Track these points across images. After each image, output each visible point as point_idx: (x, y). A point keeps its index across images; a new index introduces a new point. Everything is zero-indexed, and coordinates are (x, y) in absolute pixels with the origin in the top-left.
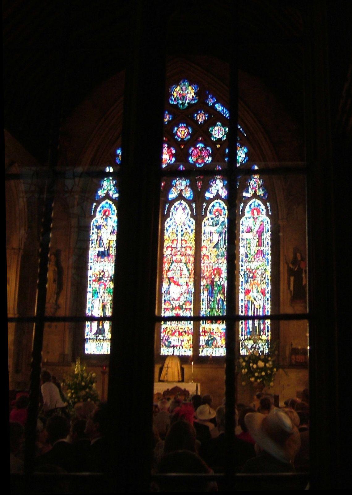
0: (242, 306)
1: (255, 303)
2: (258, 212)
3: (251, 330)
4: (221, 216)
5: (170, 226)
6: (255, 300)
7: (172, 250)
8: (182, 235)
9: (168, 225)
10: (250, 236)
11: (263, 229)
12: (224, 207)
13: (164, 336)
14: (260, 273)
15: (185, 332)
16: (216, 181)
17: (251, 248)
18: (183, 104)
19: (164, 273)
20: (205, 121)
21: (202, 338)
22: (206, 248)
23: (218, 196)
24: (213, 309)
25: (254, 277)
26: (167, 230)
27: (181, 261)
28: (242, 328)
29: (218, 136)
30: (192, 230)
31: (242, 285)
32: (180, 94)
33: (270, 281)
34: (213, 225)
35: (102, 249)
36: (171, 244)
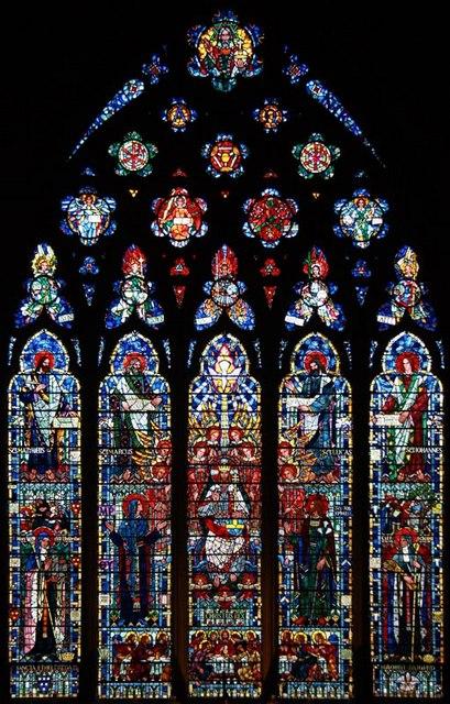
0: (375, 584)
1: (407, 578)
3: (397, 639)
4: (324, 372)
5: (200, 396)
6: (407, 571)
7: (206, 454)
8: (231, 418)
9: (198, 391)
10: (393, 420)
12: (330, 350)
13: (194, 655)
14: (418, 508)
15: (244, 644)
16: (311, 284)
17: (398, 450)
20: (281, 124)
21: (283, 659)
22: (290, 447)
23: (315, 323)
24: (307, 591)
25: (402, 519)
26: (195, 405)
27: (229, 481)
28: (376, 636)
29: (315, 168)
30: (254, 406)
31: (375, 536)
32: (216, 50)
33: (441, 527)
34: (304, 395)
36: (205, 439)
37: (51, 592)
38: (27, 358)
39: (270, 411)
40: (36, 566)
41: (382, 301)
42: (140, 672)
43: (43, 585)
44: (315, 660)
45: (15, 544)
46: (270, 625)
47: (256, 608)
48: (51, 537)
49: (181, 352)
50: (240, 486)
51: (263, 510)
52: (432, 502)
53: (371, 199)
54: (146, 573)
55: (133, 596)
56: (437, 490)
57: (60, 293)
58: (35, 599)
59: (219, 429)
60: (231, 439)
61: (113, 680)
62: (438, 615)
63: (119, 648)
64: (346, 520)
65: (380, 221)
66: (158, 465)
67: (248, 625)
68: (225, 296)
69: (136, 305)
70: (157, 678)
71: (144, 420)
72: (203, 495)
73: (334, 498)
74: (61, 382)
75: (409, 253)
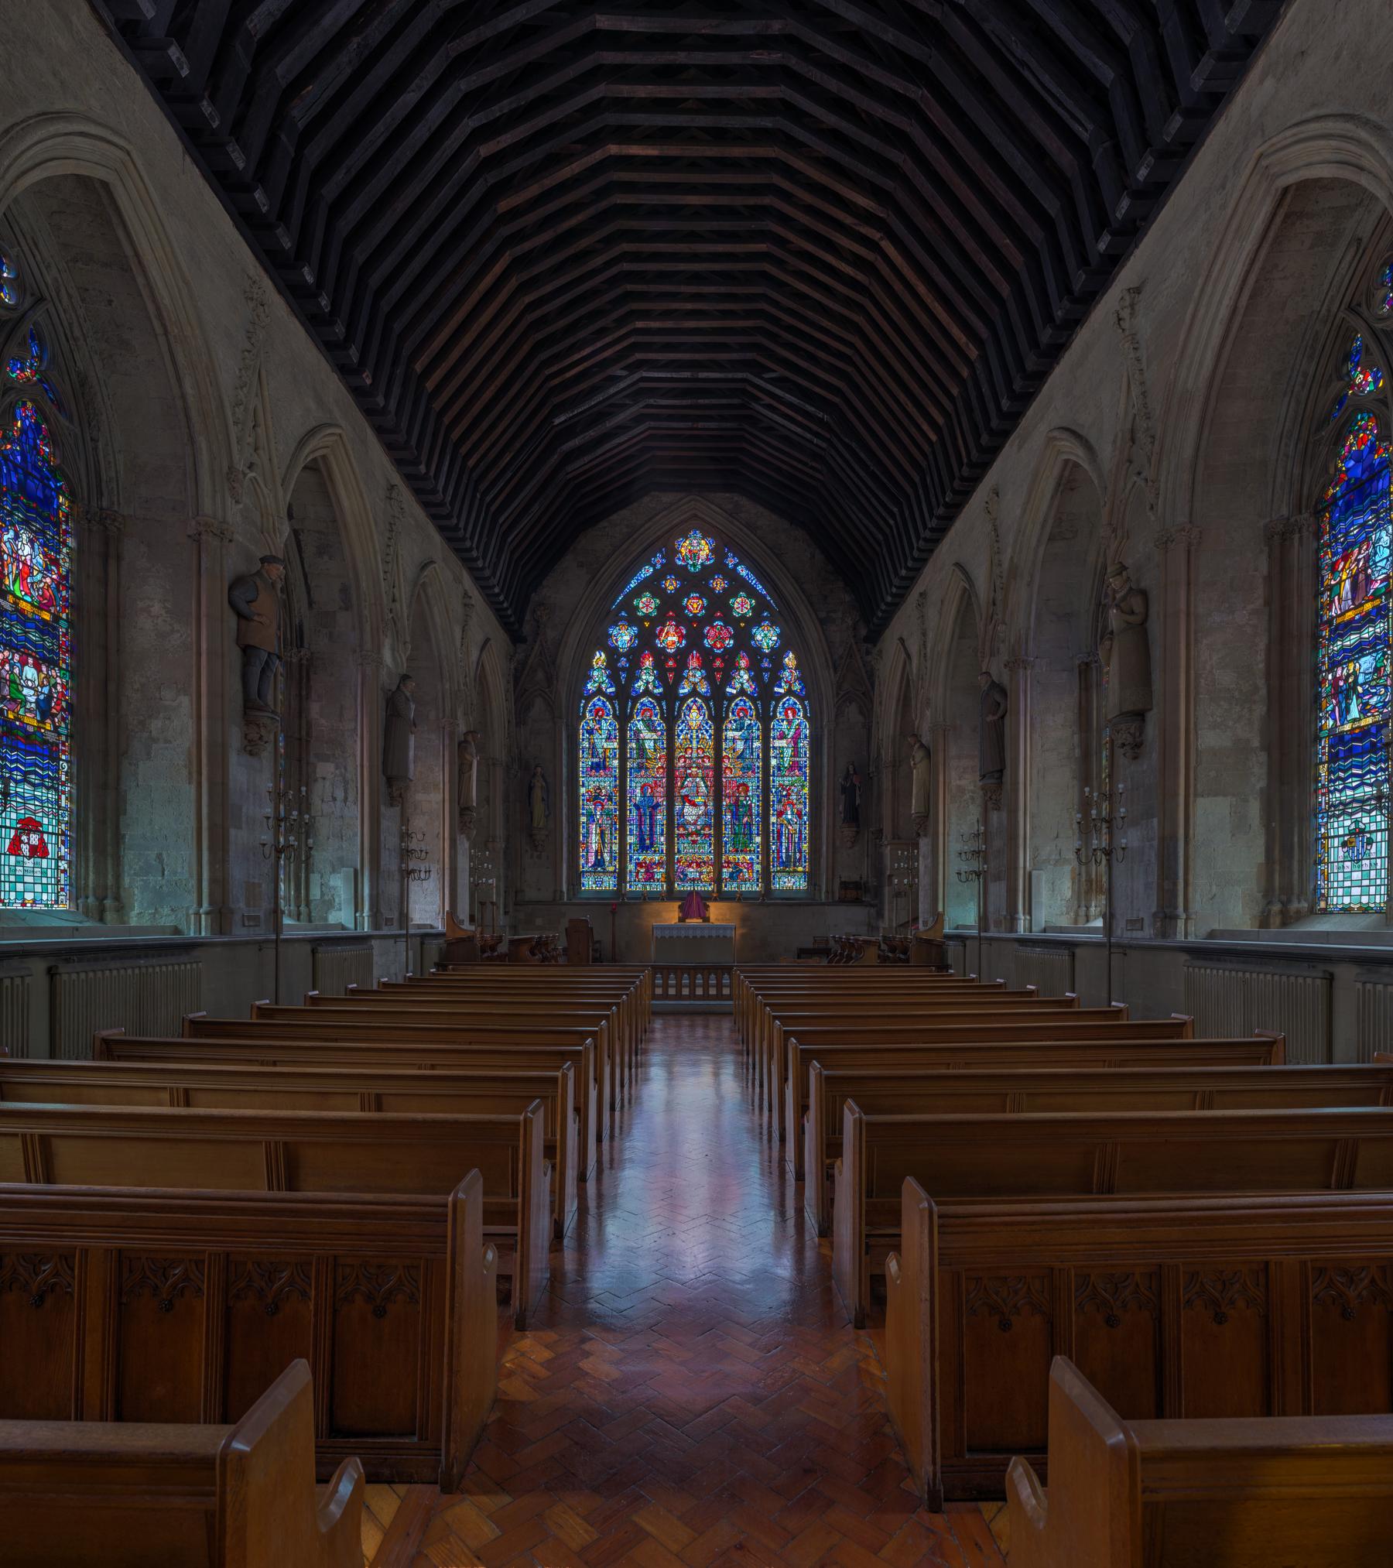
1: (790, 827)
2: (794, 714)
5: (682, 731)
6: (790, 823)
7: (685, 762)
8: (698, 742)
10: (783, 743)
11: (800, 735)
15: (704, 863)
18: (694, 565)
19: (677, 790)
20: (724, 588)
21: (725, 870)
22: (729, 758)
23: (742, 692)
25: (788, 795)
26: (679, 736)
27: (697, 776)
28: (773, 859)
32: (690, 551)
34: (736, 730)
35: (596, 760)
37: (602, 834)
38: (590, 711)
39: (718, 738)
40: (594, 821)
41: (776, 680)
42: (650, 877)
43: (598, 831)
44: (741, 871)
45: (583, 809)
46: (718, 853)
47: (710, 844)
48: (603, 805)
49: (671, 708)
50: (702, 778)
51: (715, 791)
52: (803, 786)
53: (771, 627)
54: (652, 826)
55: (646, 837)
56: (805, 780)
57: (608, 677)
58: (594, 839)
59: (692, 748)
60: (698, 754)
61: (635, 881)
62: (805, 847)
63: (639, 864)
64: (758, 796)
65: (775, 638)
66: (659, 768)
67: (706, 851)
68: (695, 677)
69: (648, 683)
70: (658, 880)
71: (652, 744)
72: (683, 784)
73: (753, 784)
74: (607, 724)
75: (791, 655)
